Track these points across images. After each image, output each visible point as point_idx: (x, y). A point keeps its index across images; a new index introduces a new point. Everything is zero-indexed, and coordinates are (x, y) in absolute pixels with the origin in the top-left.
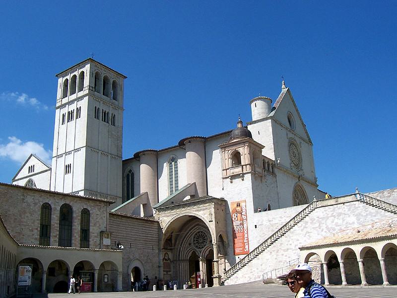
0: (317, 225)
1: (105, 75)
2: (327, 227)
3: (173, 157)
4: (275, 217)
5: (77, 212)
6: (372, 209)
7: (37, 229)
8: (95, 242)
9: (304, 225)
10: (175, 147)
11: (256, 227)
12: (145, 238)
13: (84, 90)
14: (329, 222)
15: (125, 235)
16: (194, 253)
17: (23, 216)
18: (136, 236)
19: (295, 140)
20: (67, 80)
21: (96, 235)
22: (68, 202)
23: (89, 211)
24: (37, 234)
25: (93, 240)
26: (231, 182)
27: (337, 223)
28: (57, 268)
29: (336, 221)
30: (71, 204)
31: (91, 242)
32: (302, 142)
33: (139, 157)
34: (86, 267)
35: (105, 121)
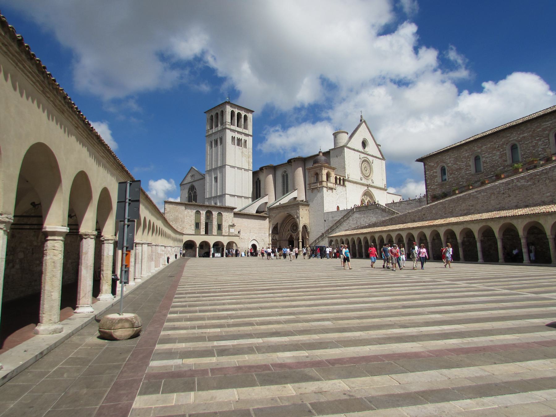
2: (360, 223)
3: (285, 170)
4: (336, 215)
5: (215, 214)
6: (385, 214)
7: (193, 225)
8: (226, 231)
9: (348, 221)
10: (286, 163)
12: (259, 226)
13: (223, 124)
15: (246, 225)
16: (291, 236)
18: (254, 226)
19: (367, 158)
20: (212, 116)
21: (226, 227)
22: (209, 209)
23: (222, 214)
24: (193, 227)
25: (224, 230)
26: (312, 192)
27: (366, 221)
28: (204, 245)
29: (365, 220)
30: (211, 210)
31: (223, 231)
32: (374, 159)
33: (263, 170)
34: (220, 245)
35: (239, 145)
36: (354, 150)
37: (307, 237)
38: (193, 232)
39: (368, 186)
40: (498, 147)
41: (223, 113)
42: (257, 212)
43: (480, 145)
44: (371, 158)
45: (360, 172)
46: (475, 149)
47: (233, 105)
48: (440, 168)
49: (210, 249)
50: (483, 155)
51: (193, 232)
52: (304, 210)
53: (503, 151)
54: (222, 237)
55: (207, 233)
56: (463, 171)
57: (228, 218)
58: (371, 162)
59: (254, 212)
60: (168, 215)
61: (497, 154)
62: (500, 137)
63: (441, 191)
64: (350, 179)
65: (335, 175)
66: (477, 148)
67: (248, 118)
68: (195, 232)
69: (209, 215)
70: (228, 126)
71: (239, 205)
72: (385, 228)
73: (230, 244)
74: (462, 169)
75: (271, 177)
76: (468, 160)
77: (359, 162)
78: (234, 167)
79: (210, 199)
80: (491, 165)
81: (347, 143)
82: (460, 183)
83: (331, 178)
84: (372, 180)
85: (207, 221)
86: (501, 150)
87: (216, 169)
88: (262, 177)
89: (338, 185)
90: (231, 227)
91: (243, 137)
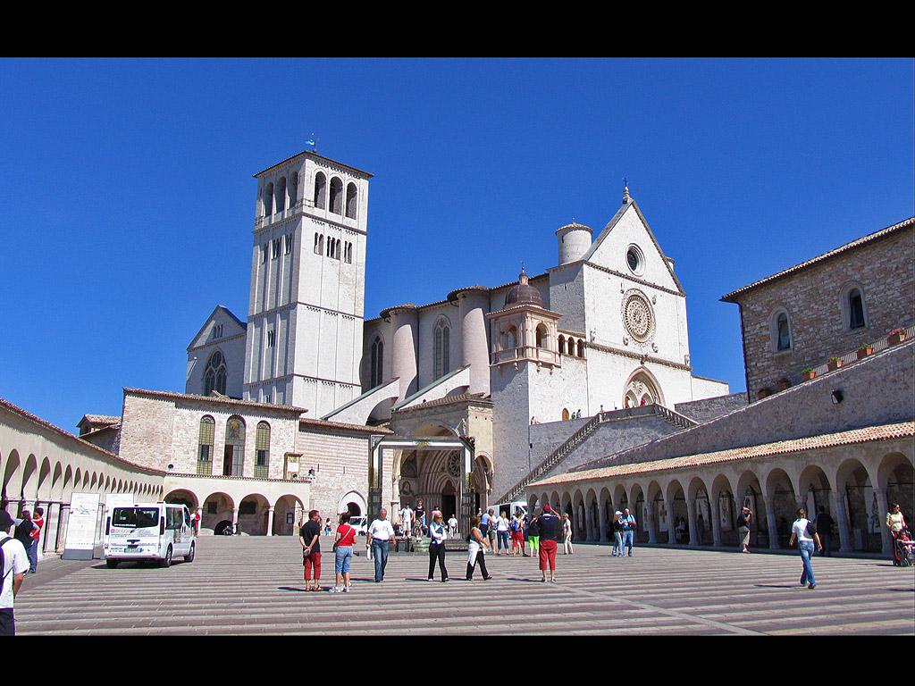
0: (602, 449)
1: (334, 175)
7: (194, 450)
11: (531, 447)
14: (617, 445)
17: (175, 434)
24: (194, 456)
29: (626, 444)
34: (261, 504)
36: (607, 271)
37: (488, 488)
38: (194, 471)
39: (644, 359)
40: (897, 268)
41: (296, 180)
42: (372, 421)
43: (859, 264)
44: (649, 292)
45: (622, 325)
46: (849, 273)
47: (319, 159)
48: (776, 317)
49: (233, 512)
50: (866, 288)
51: (194, 471)
52: (481, 419)
53: (908, 277)
54: (265, 483)
55: (227, 472)
56: (826, 325)
57: (284, 434)
58: (651, 300)
59: (361, 421)
60: (131, 423)
61: (895, 285)
62: (899, 245)
63: (779, 373)
64: (595, 342)
65: (558, 331)
66: (853, 270)
67: (358, 192)
68: (198, 470)
69: (236, 431)
70: (305, 210)
71: (311, 400)
72: (646, 467)
73: (287, 502)
74: (824, 319)
75: (406, 332)
76: (835, 298)
77: (619, 300)
78: (318, 309)
79: (254, 388)
80: (884, 312)
81: (591, 254)
82: (820, 355)
83: (549, 338)
84: (653, 344)
85: (230, 443)
86: (904, 275)
87: (271, 316)
88: (385, 331)
89: (566, 356)
90: (292, 458)
91: (343, 236)
